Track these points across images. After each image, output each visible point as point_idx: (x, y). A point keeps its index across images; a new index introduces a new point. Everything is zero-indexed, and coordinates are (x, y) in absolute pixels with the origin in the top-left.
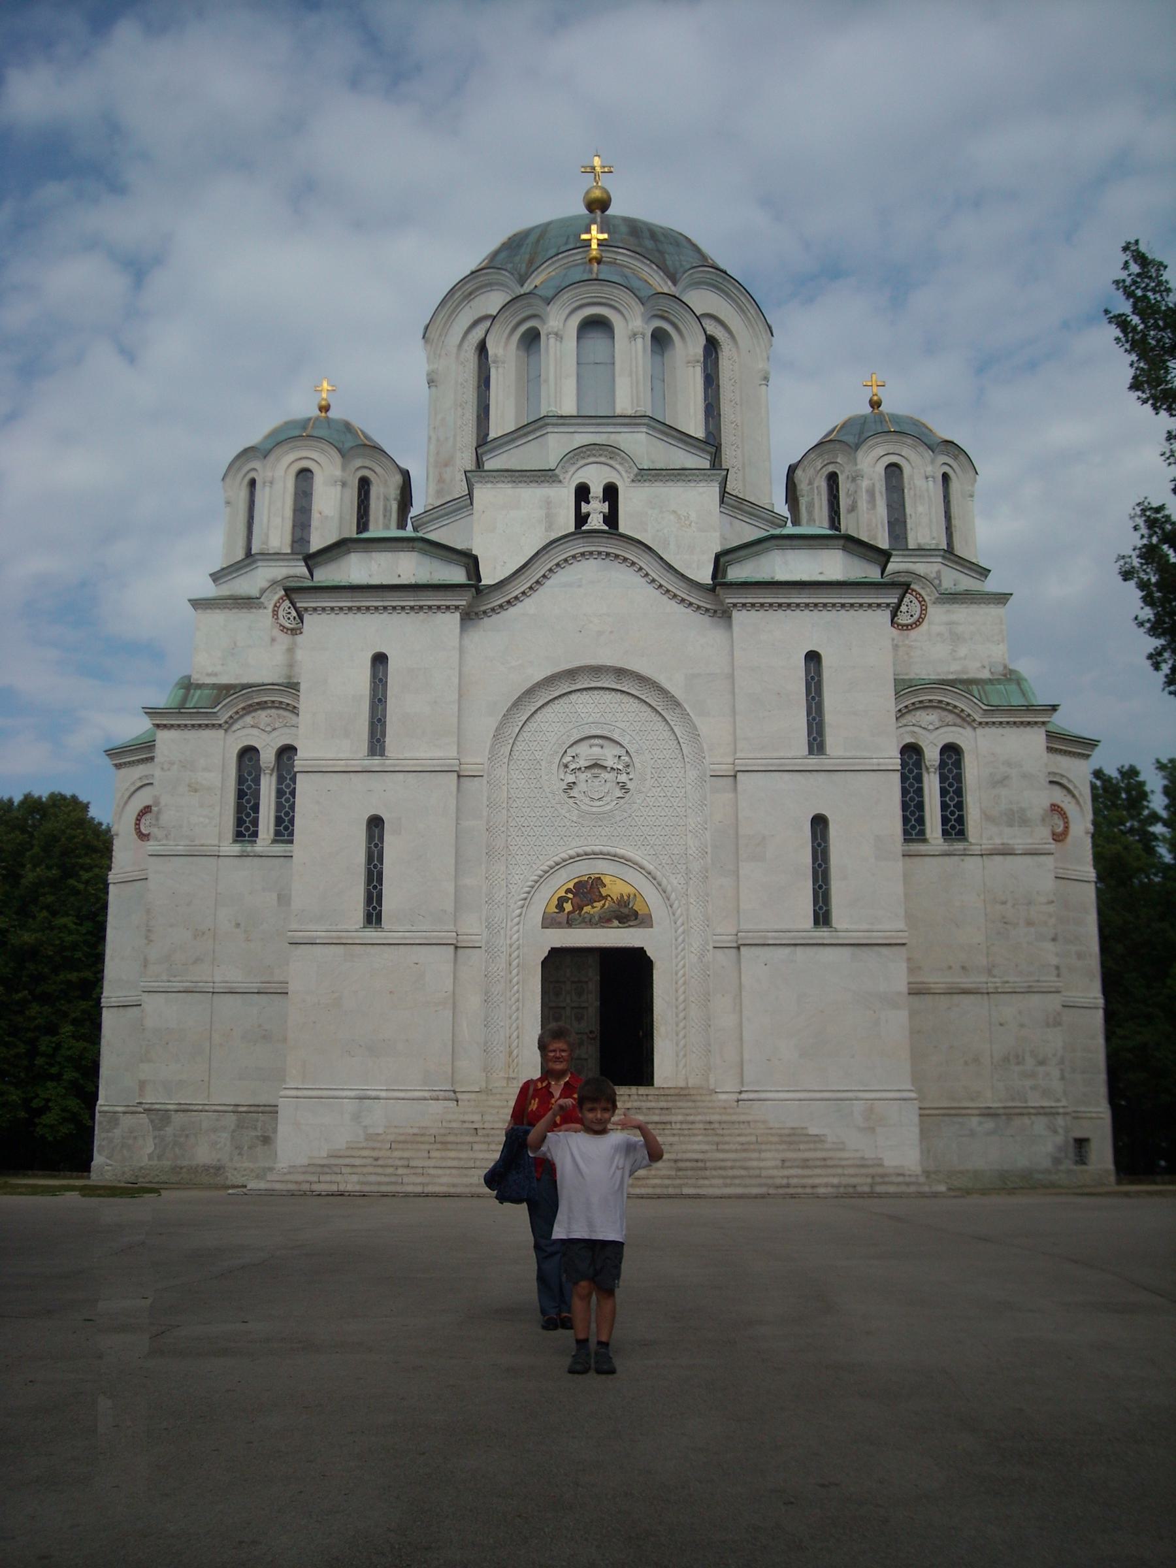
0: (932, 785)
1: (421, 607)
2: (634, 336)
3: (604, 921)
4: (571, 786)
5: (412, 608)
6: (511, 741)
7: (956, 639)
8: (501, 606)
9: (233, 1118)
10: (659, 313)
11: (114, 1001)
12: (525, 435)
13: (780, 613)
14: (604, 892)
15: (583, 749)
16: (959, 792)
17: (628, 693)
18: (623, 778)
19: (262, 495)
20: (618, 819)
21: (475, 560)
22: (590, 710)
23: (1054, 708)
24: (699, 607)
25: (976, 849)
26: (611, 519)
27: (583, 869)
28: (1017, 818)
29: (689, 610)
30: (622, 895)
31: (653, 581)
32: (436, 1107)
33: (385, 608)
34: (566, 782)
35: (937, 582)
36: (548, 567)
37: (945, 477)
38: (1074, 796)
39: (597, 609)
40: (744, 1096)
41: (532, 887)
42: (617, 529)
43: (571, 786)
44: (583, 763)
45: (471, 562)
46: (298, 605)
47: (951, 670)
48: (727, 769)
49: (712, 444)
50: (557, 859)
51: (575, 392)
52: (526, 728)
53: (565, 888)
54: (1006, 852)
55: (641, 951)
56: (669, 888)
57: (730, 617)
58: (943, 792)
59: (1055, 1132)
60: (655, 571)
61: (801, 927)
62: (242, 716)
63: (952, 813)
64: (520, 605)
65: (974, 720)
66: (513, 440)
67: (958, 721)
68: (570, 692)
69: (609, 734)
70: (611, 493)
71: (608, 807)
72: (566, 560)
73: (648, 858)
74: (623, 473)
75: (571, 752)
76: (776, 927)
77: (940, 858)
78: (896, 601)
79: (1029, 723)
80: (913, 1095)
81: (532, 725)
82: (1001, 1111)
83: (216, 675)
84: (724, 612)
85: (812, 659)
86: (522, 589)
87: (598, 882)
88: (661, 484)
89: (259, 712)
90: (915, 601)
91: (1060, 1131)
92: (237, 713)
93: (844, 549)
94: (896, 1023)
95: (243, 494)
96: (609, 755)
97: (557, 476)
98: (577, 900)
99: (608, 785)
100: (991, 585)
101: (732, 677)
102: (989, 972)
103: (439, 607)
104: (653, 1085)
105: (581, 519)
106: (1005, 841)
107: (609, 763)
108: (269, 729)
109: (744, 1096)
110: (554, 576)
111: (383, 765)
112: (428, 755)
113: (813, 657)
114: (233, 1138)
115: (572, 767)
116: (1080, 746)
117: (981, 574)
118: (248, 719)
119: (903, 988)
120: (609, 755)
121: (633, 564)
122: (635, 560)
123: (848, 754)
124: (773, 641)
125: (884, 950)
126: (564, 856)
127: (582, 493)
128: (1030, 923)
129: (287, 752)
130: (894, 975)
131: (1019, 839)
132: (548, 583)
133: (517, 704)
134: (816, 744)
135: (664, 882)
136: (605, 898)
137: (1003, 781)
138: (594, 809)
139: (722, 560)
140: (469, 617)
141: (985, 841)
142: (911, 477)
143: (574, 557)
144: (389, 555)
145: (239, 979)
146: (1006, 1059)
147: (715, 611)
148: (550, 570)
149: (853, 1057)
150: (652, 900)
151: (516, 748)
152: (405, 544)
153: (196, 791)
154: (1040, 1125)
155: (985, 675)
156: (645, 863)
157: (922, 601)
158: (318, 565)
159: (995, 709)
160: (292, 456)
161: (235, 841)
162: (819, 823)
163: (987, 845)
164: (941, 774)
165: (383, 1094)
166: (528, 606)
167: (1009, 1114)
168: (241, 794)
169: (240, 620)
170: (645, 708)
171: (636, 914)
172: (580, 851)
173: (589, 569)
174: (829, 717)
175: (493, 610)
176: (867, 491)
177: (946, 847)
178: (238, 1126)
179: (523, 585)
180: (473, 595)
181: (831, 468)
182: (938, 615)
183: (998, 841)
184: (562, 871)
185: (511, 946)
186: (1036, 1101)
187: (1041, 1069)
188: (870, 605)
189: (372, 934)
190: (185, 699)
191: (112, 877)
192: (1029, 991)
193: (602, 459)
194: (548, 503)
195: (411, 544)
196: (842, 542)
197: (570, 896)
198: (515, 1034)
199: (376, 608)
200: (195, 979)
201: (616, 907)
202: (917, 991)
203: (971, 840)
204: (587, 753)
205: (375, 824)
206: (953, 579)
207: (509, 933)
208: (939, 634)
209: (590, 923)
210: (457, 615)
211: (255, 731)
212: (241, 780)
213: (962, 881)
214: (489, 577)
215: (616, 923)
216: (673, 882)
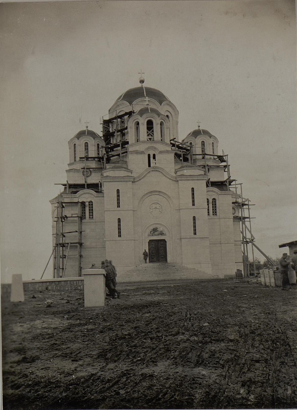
0: (211, 205)
2: (157, 124)
19: (77, 148)
22: (155, 198)
27: (154, 226)
37: (213, 143)
70: (154, 156)
95: (73, 147)
96: (158, 206)
124: (186, 186)
127: (149, 156)
129: (91, 203)
140: (133, 182)
150: (165, 231)
204: (154, 206)
205: (119, 220)
209: (156, 235)
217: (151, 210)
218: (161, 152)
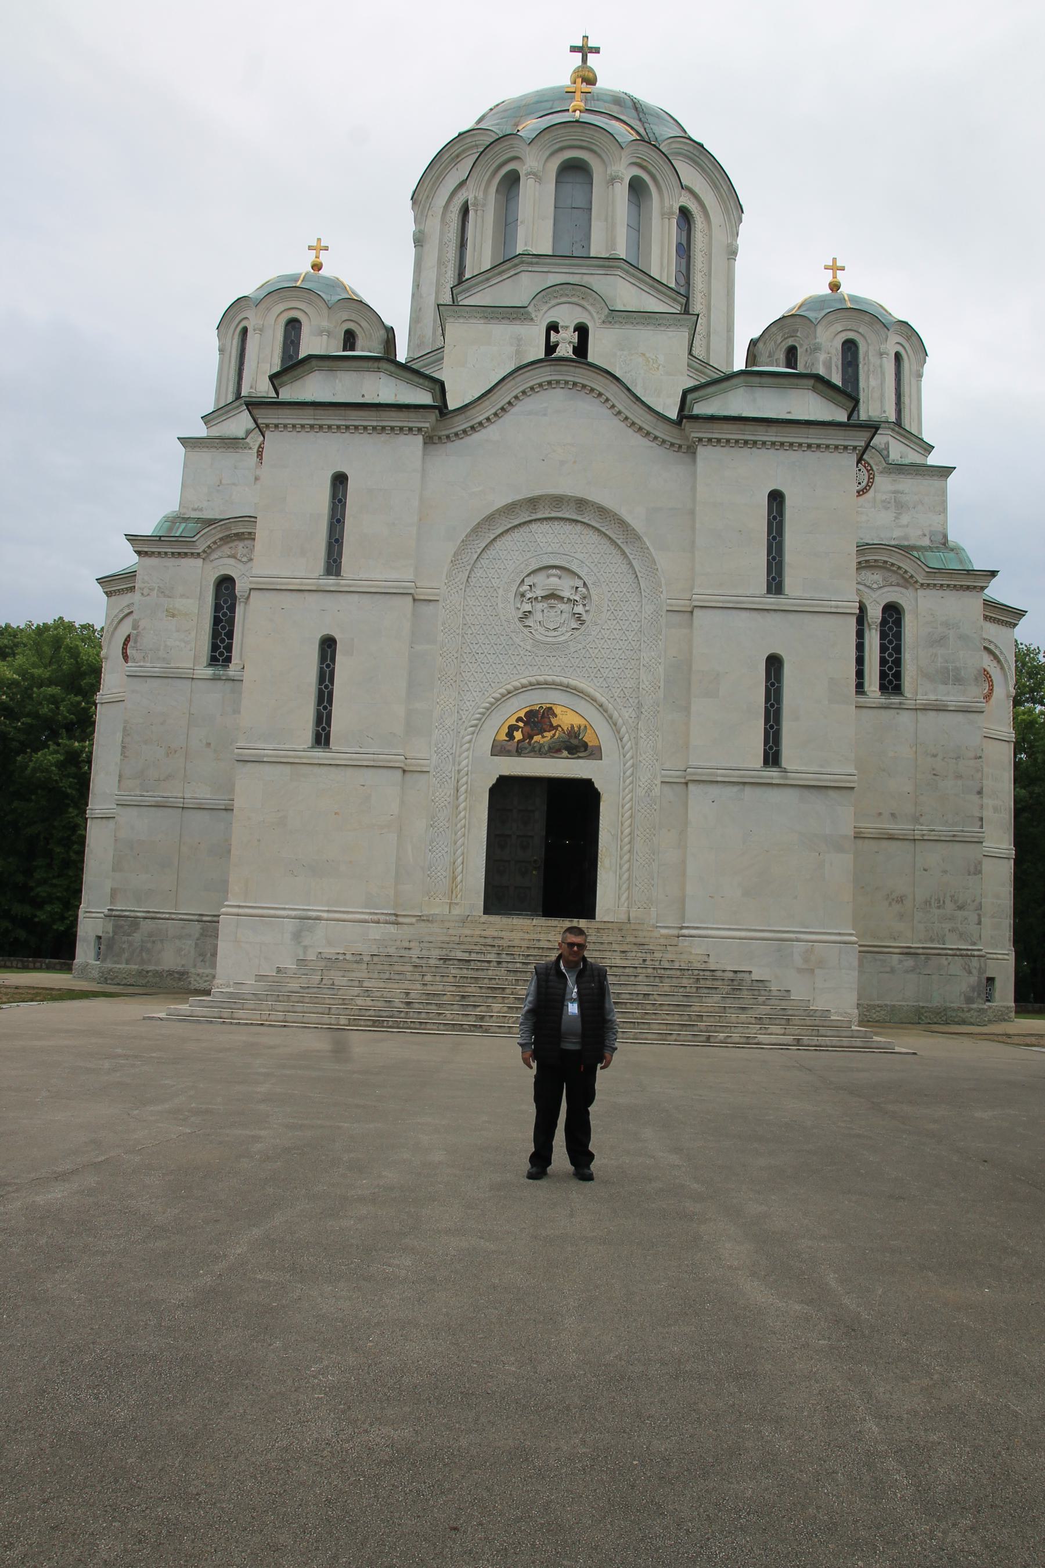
1: (383, 428)
3: (553, 751)
4: (527, 614)
5: (374, 428)
6: (469, 568)
7: (900, 507)
8: (464, 431)
9: (198, 926)
10: (638, 161)
11: (98, 813)
12: (500, 273)
13: (746, 451)
14: (555, 722)
15: (540, 579)
16: (898, 649)
17: (588, 525)
18: (579, 609)
20: (573, 650)
21: (442, 384)
22: (550, 541)
23: (993, 574)
24: (664, 441)
25: (910, 704)
26: (581, 349)
27: (537, 699)
28: (952, 676)
29: (654, 444)
30: (572, 726)
31: (619, 413)
32: (376, 932)
33: (347, 427)
34: (522, 611)
35: (885, 453)
36: (514, 394)
37: (898, 357)
38: (999, 662)
39: (560, 442)
40: (685, 932)
41: (483, 714)
42: (586, 358)
43: (527, 614)
44: (539, 593)
45: (437, 388)
46: (260, 421)
47: (894, 535)
48: (682, 604)
49: (683, 295)
50: (509, 687)
51: (551, 234)
52: (485, 556)
53: (515, 717)
54: (940, 708)
55: (588, 784)
56: (620, 721)
57: (695, 453)
58: (883, 649)
59: (970, 972)
60: (621, 401)
61: (751, 766)
62: (219, 546)
63: (890, 669)
64: (484, 431)
65: (916, 582)
66: (488, 279)
67: (901, 581)
68: (530, 521)
69: (567, 565)
70: (582, 331)
71: (563, 638)
72: (532, 388)
73: (600, 690)
74: (595, 314)
75: (529, 581)
76: (728, 765)
77: (876, 711)
78: (863, 444)
79: (968, 588)
80: (854, 939)
81: (491, 553)
82: (920, 951)
83: (201, 510)
84: (689, 447)
85: (775, 499)
86: (486, 415)
87: (550, 711)
88: (631, 327)
89: (236, 543)
90: (863, 469)
91: (975, 972)
92: (215, 543)
93: (814, 389)
94: (839, 866)
97: (528, 313)
98: (527, 729)
99: (565, 615)
100: (932, 460)
101: (692, 513)
102: (916, 819)
103: (401, 429)
104: (594, 918)
105: (550, 348)
106: (939, 697)
107: (566, 594)
108: (245, 559)
109: (685, 932)
110: (520, 404)
111: (338, 585)
112: (383, 578)
113: (776, 498)
114: (196, 944)
115: (529, 596)
116: (1007, 616)
117: (925, 450)
118: (226, 550)
119: (852, 834)
120: (565, 586)
121: (600, 395)
122: (602, 391)
123: (807, 596)
125: (832, 793)
126: (517, 684)
128: (959, 777)
130: (844, 817)
131: (952, 696)
132: (514, 410)
133: (477, 530)
134: (775, 584)
135: (616, 715)
136: (556, 728)
137: (941, 641)
138: (550, 639)
139: (689, 397)
140: (431, 440)
141: (919, 697)
142: (867, 353)
143: (540, 385)
144: (354, 374)
145: (209, 796)
146: (927, 902)
147: (680, 446)
148: (516, 397)
149: (796, 897)
150: (601, 733)
151: (473, 575)
152: (370, 364)
153: (173, 616)
154: (956, 966)
155: (926, 542)
156: (598, 696)
157: (870, 470)
158: (282, 385)
159: (939, 571)
160: (281, 307)
161: (210, 665)
162: (774, 664)
163: (922, 699)
164: (881, 631)
165: (325, 915)
166: (491, 432)
167: (928, 955)
168: (217, 621)
169: (226, 460)
170: (604, 541)
171: (585, 746)
172: (533, 680)
173: (556, 398)
174: (789, 557)
175: (456, 434)
176: (824, 363)
177: (883, 700)
178: (202, 935)
179: (487, 410)
180: (438, 419)
181: (790, 342)
182: (883, 484)
183: (933, 698)
184: (514, 700)
185: (459, 771)
186: (953, 943)
187: (959, 913)
188: (836, 447)
189: (320, 754)
190: (170, 529)
191: (98, 698)
192: (953, 840)
193: (574, 300)
194: (519, 340)
195: (376, 365)
196: (811, 382)
197: (521, 724)
198: (460, 860)
199: (338, 427)
200: (165, 795)
201: (566, 738)
202: (858, 836)
203: (908, 694)
204: (545, 583)
205: (328, 645)
206: (898, 451)
207: (457, 759)
208: (884, 501)
210: (420, 439)
211: (232, 561)
212: (217, 608)
213: (905, 731)
214: (452, 405)
215: (565, 753)
216: (625, 715)
217: (527, 607)
218: (616, 316)
